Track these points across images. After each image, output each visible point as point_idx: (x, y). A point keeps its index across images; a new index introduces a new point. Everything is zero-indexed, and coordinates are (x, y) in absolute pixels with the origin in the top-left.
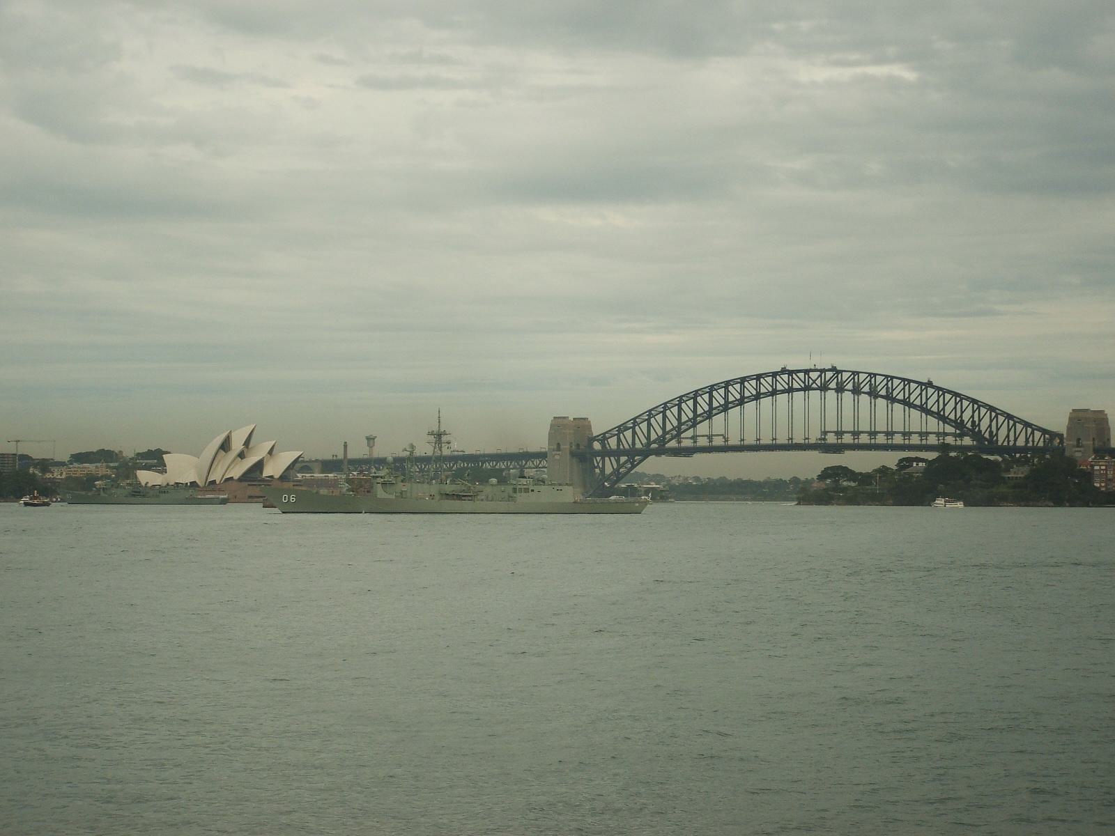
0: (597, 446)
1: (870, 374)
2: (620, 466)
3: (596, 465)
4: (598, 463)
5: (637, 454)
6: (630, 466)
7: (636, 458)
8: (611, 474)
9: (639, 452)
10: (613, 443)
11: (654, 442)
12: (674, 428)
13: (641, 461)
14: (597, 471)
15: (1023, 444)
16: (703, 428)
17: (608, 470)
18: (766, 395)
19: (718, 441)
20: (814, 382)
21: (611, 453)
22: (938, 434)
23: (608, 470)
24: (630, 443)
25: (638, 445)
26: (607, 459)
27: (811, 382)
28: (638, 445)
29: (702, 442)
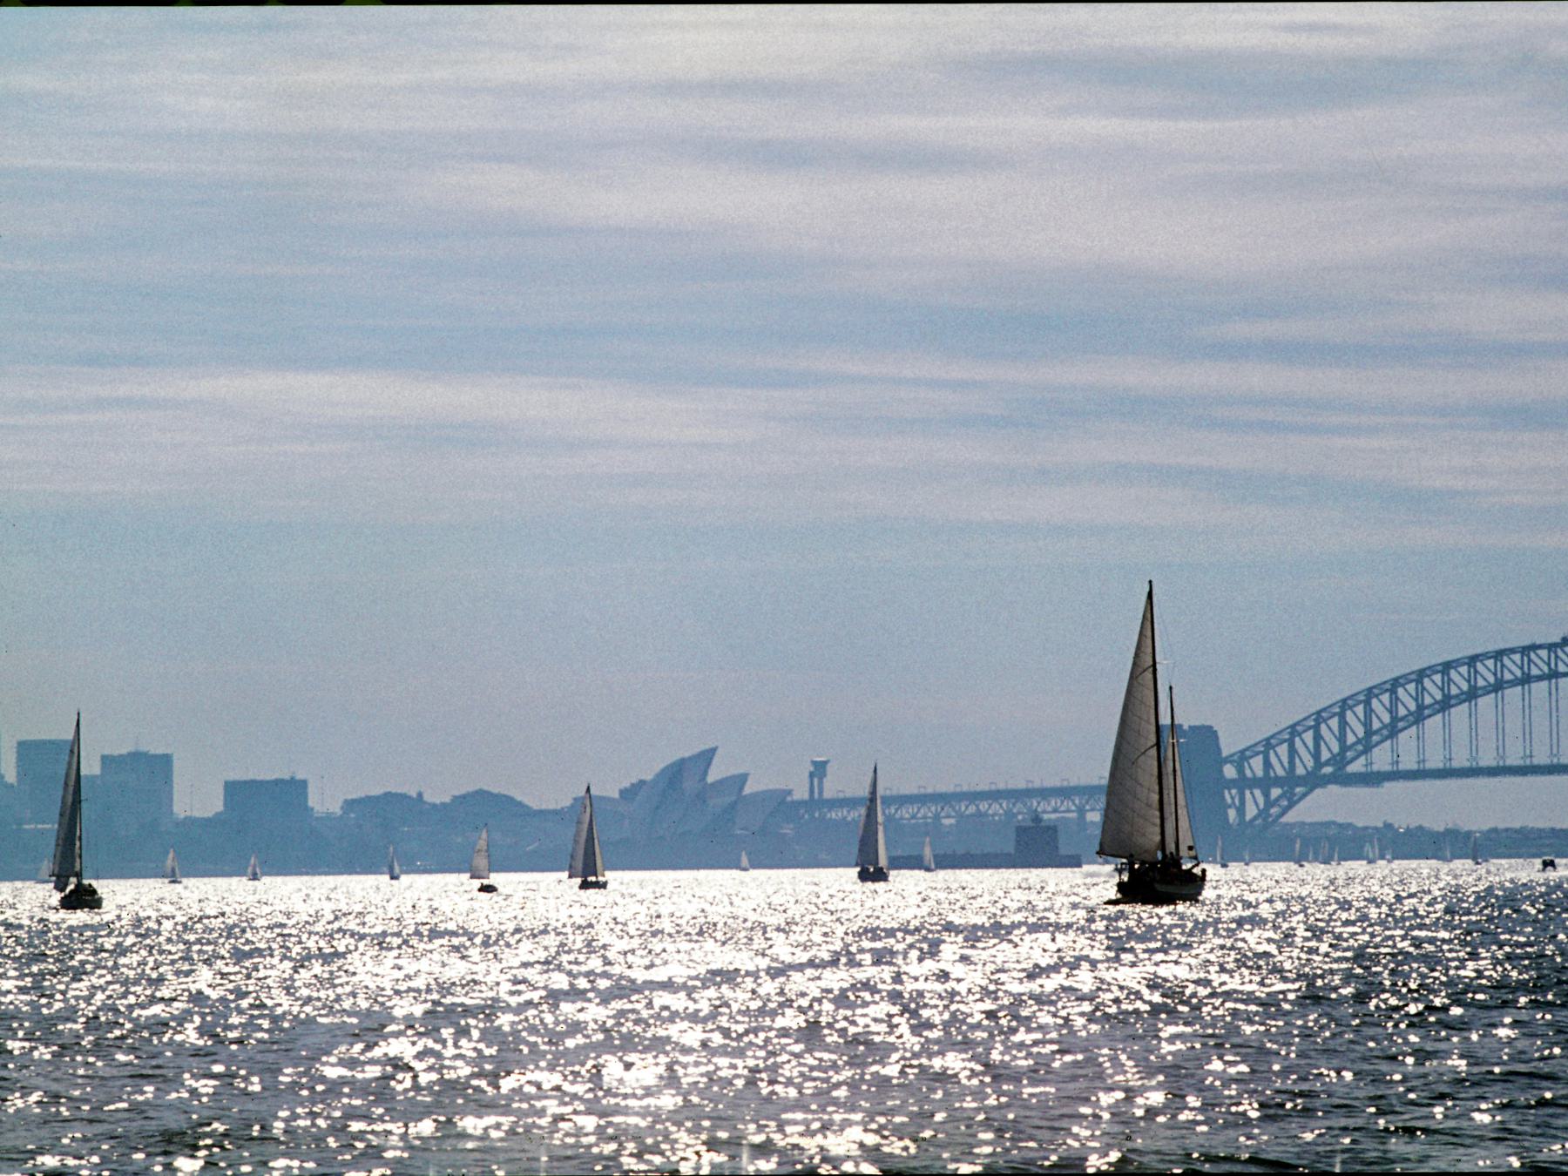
0: (1230, 772)
2: (1269, 804)
3: (1229, 800)
4: (1232, 798)
5: (1297, 785)
6: (1286, 803)
8: (1255, 818)
9: (1301, 781)
10: (1257, 764)
11: (1327, 763)
13: (1305, 795)
14: (1232, 813)
16: (1407, 737)
17: (1251, 811)
21: (1255, 783)
23: (1251, 811)
25: (1300, 771)
26: (1247, 793)
28: (1300, 771)
29: (1408, 763)
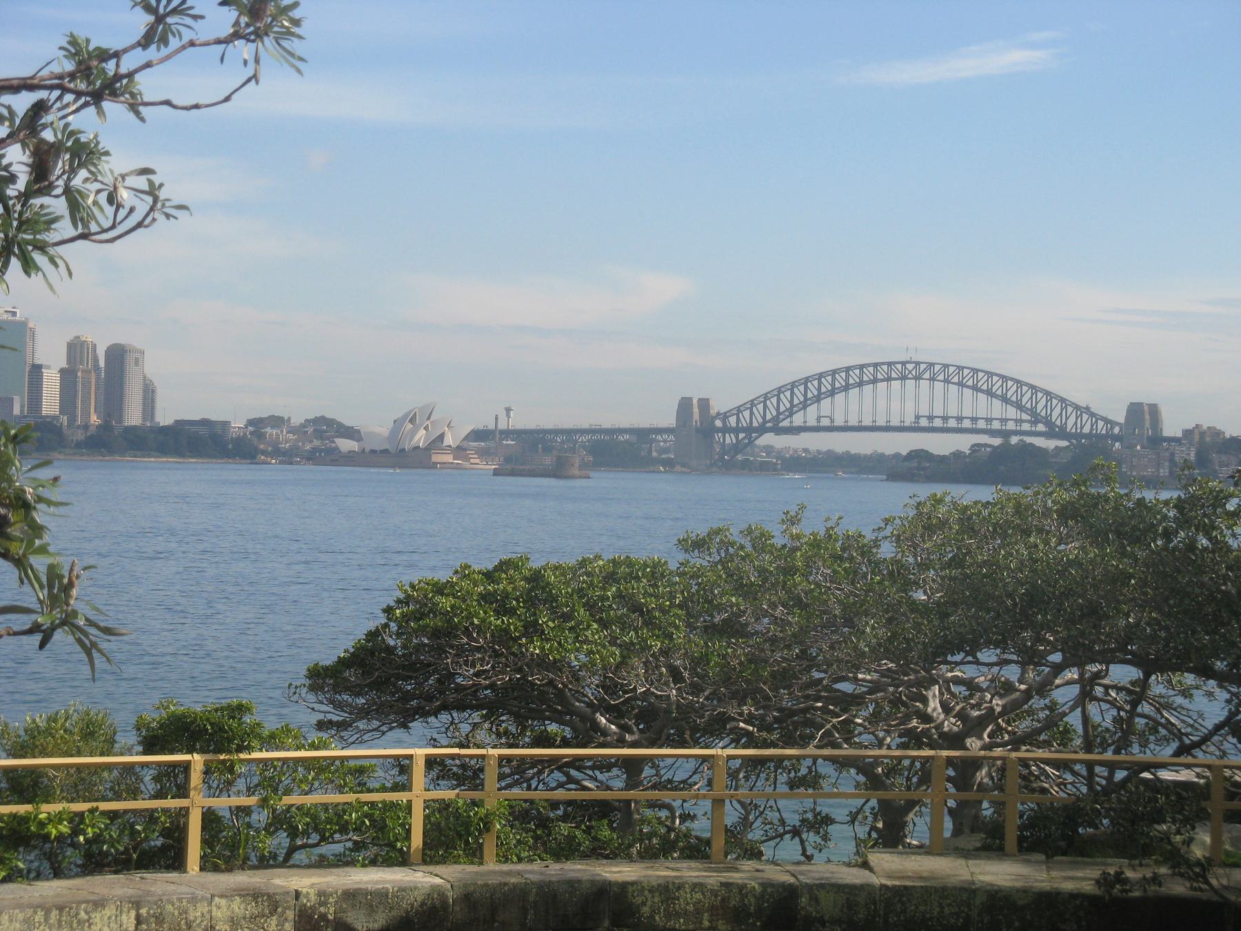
0: (718, 423)
1: (958, 367)
7: (753, 435)
9: (756, 430)
10: (732, 421)
11: (769, 421)
12: (787, 410)
15: (1088, 431)
16: (812, 410)
18: (868, 383)
19: (825, 422)
20: (910, 372)
22: (1016, 421)
24: (748, 421)
26: (727, 435)
27: (907, 372)
28: (755, 424)
29: (812, 422)
